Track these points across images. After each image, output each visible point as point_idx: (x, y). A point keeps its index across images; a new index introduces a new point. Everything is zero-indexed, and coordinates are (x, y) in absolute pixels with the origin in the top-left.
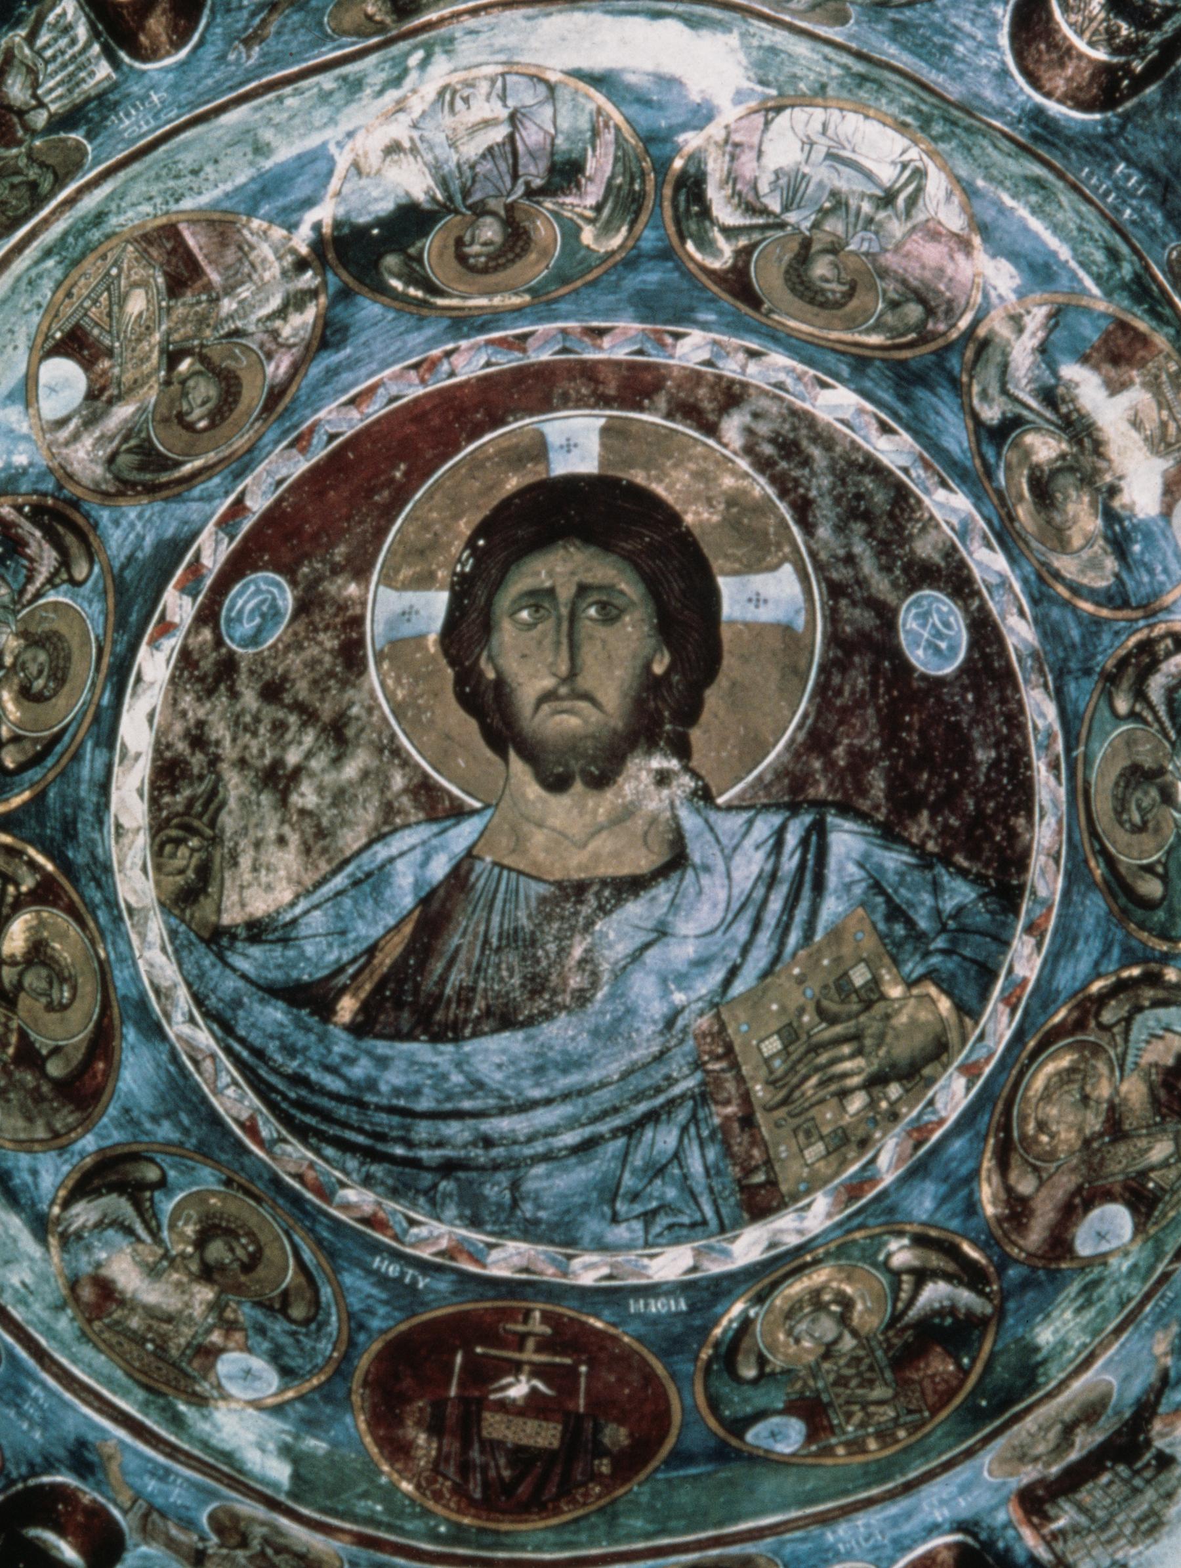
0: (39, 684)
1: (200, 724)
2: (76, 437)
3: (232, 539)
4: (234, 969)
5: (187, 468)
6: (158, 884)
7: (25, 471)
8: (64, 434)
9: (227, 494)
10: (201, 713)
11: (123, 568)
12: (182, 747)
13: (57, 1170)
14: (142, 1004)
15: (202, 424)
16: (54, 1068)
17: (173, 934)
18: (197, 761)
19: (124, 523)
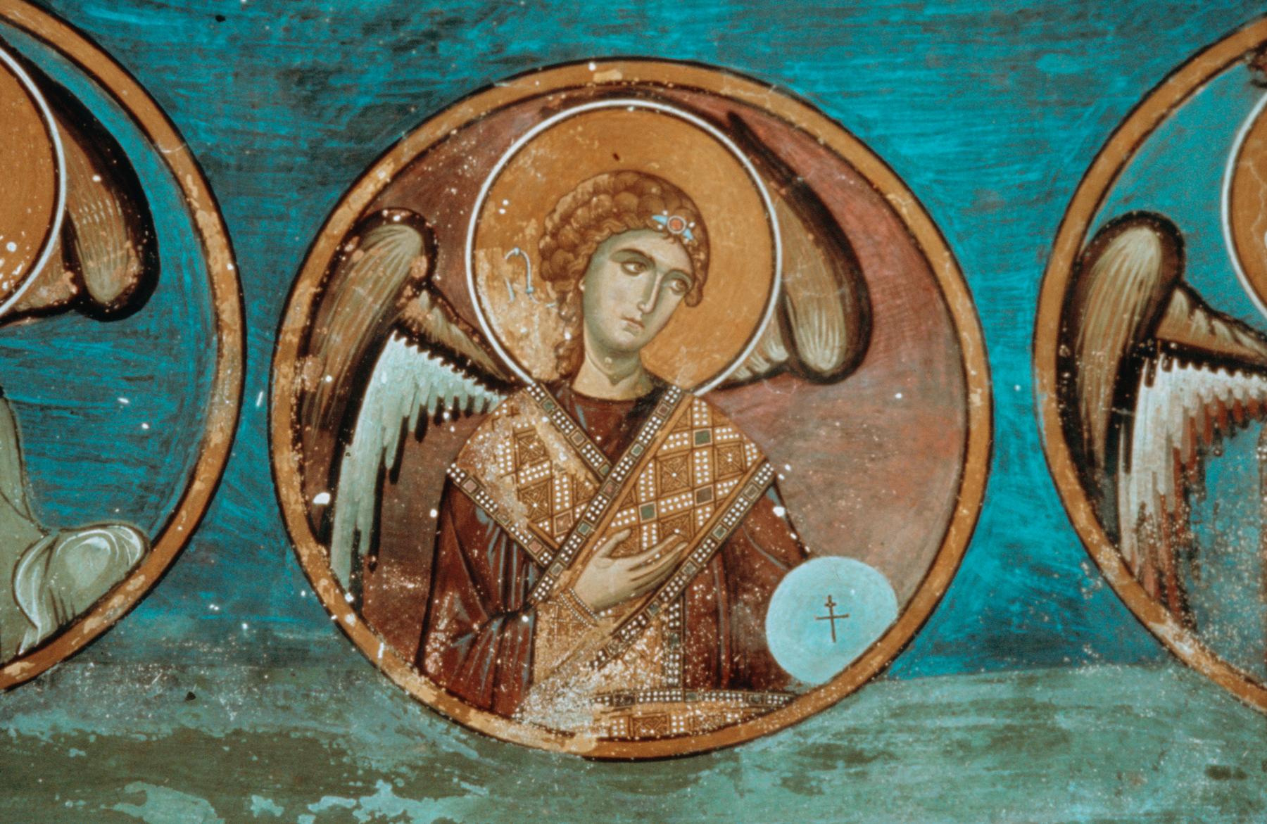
13: (1029, 494)
16: (823, 347)
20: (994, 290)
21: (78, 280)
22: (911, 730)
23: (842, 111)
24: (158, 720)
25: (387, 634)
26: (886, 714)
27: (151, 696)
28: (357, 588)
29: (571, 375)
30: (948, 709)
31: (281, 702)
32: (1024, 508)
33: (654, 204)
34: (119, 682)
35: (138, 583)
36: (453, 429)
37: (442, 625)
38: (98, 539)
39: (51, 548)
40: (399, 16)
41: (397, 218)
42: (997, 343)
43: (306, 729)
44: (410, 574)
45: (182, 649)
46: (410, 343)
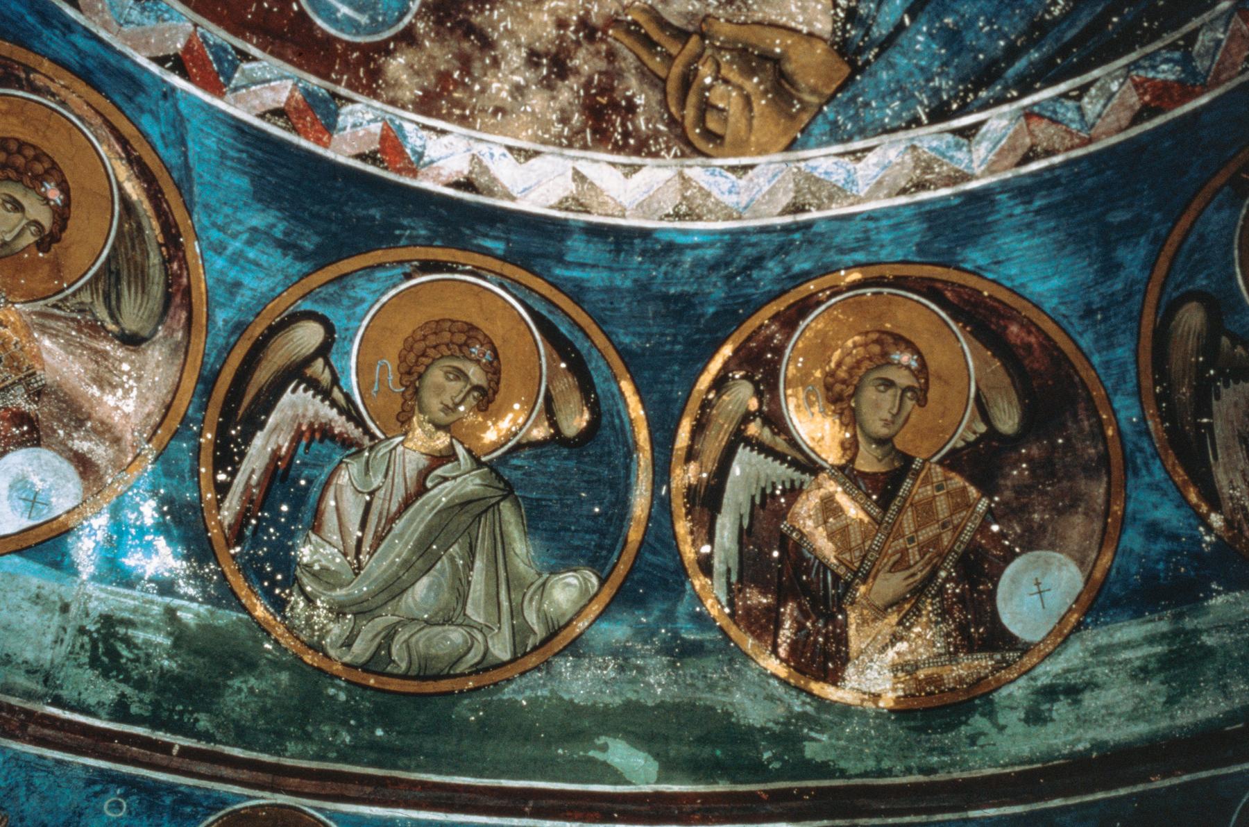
0: (476, 374)
1: (533, 59)
2: (106, 432)
3: (246, 57)
4: (900, 28)
5: (134, 190)
6: (762, 151)
7: (163, 501)
8: (100, 452)
9: (170, 93)
10: (516, 58)
11: (302, 256)
12: (567, 92)
13: (1154, 487)
14: (933, 216)
15: (55, 195)
16: (1008, 421)
17: (836, 135)
18: (584, 62)
19: (232, 274)
20: (1107, 362)
21: (553, 424)
22: (1104, 663)
23: (995, 272)
24: (614, 693)
25: (753, 633)
26: (1087, 654)
27: (607, 678)
28: (731, 603)
29: (852, 460)
30: (1127, 645)
31: (689, 681)
32: (1154, 497)
33: (891, 349)
34: (588, 669)
35: (596, 608)
36: (783, 500)
37: (787, 625)
38: (571, 579)
39: (544, 584)
40: (729, 259)
41: (737, 376)
42: (1116, 394)
43: (706, 699)
44: (764, 595)
45: (625, 647)
46: (752, 450)
